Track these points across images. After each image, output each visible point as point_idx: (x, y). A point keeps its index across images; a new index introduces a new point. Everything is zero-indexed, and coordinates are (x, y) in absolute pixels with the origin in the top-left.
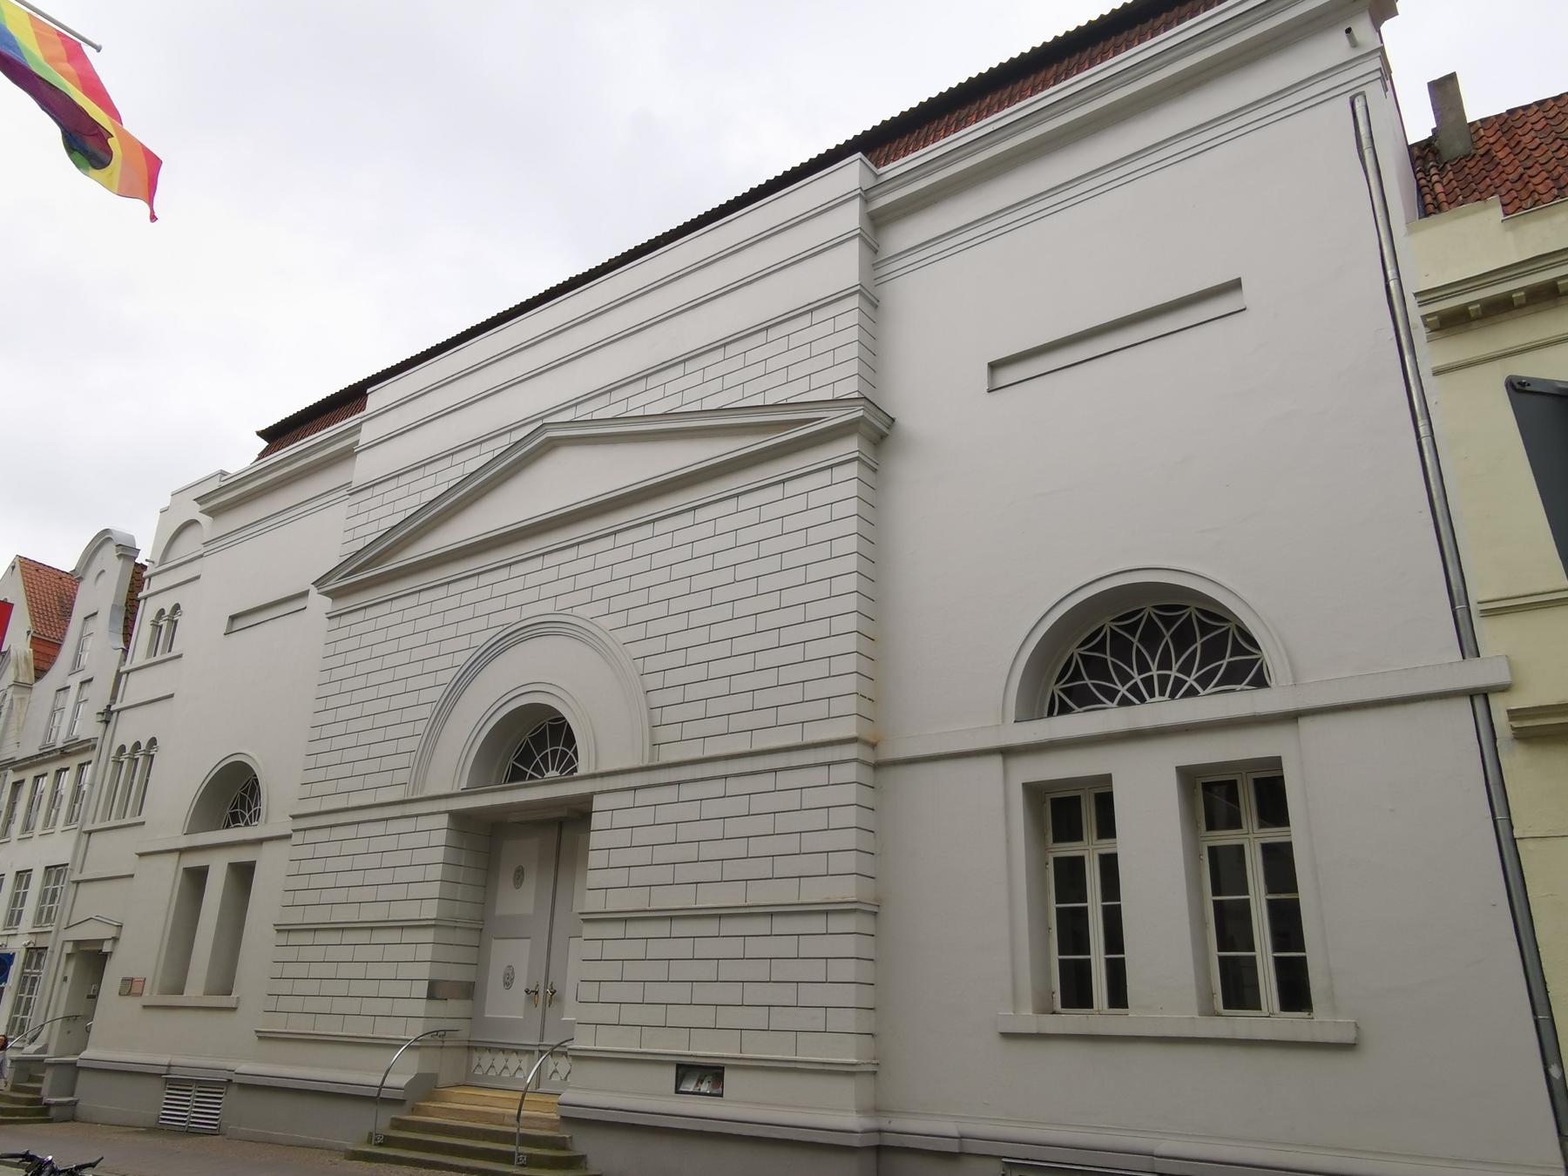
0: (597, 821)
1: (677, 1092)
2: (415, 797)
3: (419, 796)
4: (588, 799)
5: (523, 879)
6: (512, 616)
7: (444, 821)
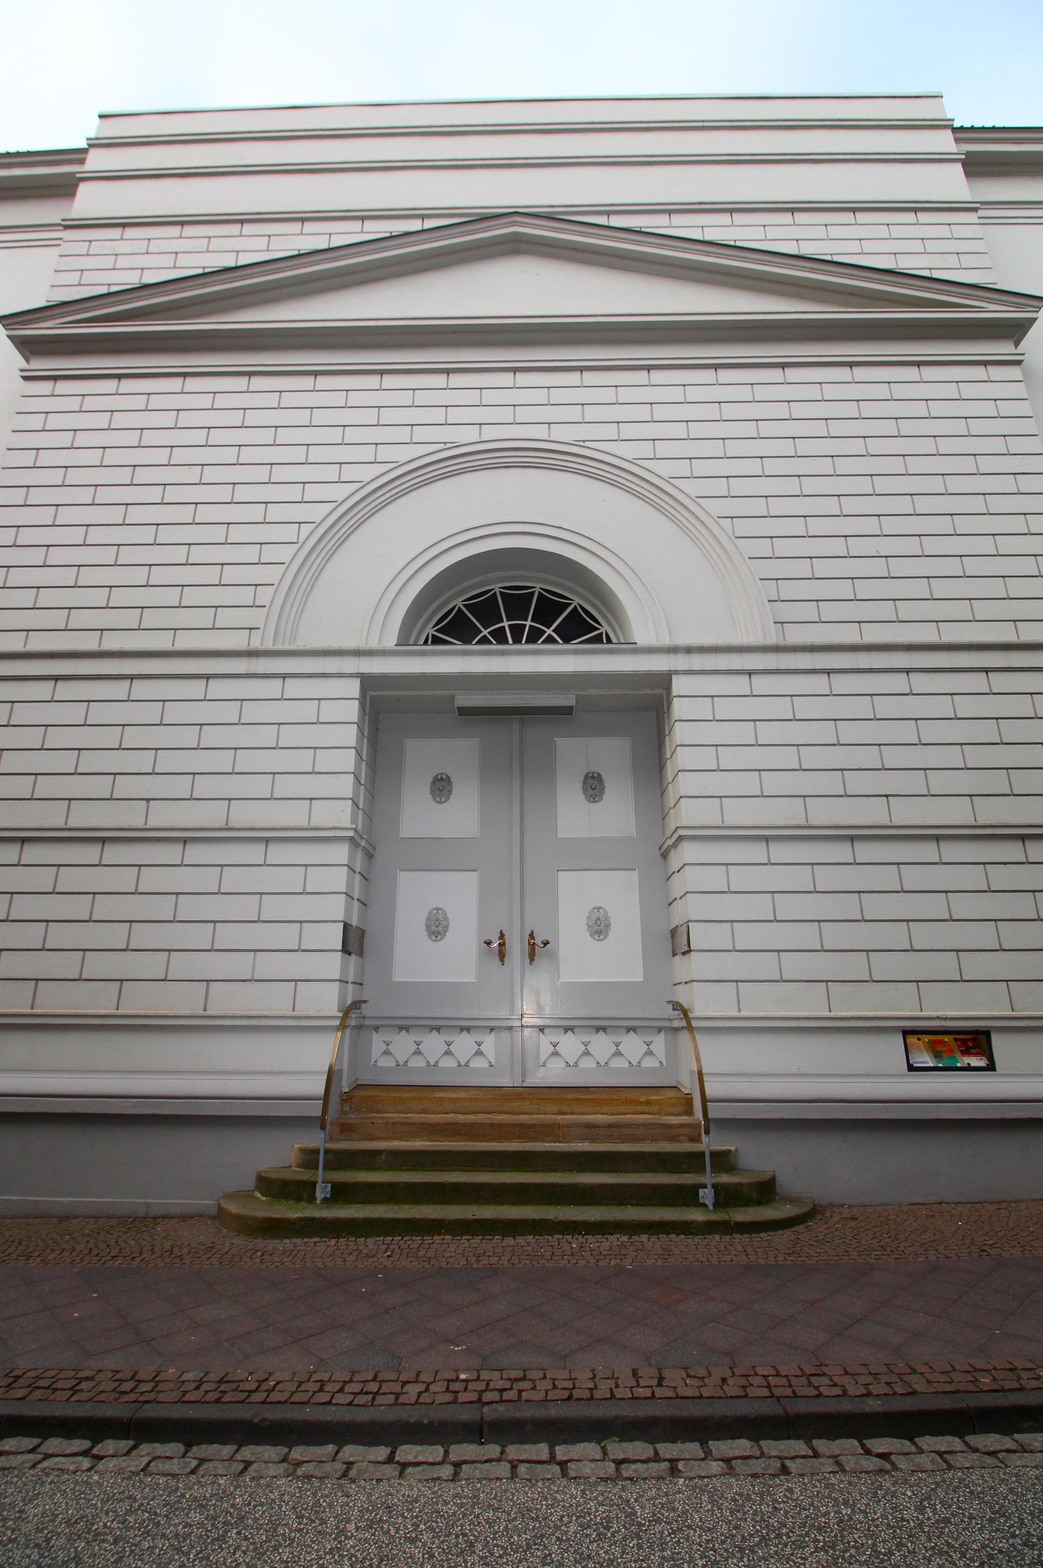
0: (680, 708)
1: (911, 1068)
2: (279, 647)
3: (286, 647)
4: (664, 680)
5: (450, 792)
6: (470, 435)
7: (354, 687)
